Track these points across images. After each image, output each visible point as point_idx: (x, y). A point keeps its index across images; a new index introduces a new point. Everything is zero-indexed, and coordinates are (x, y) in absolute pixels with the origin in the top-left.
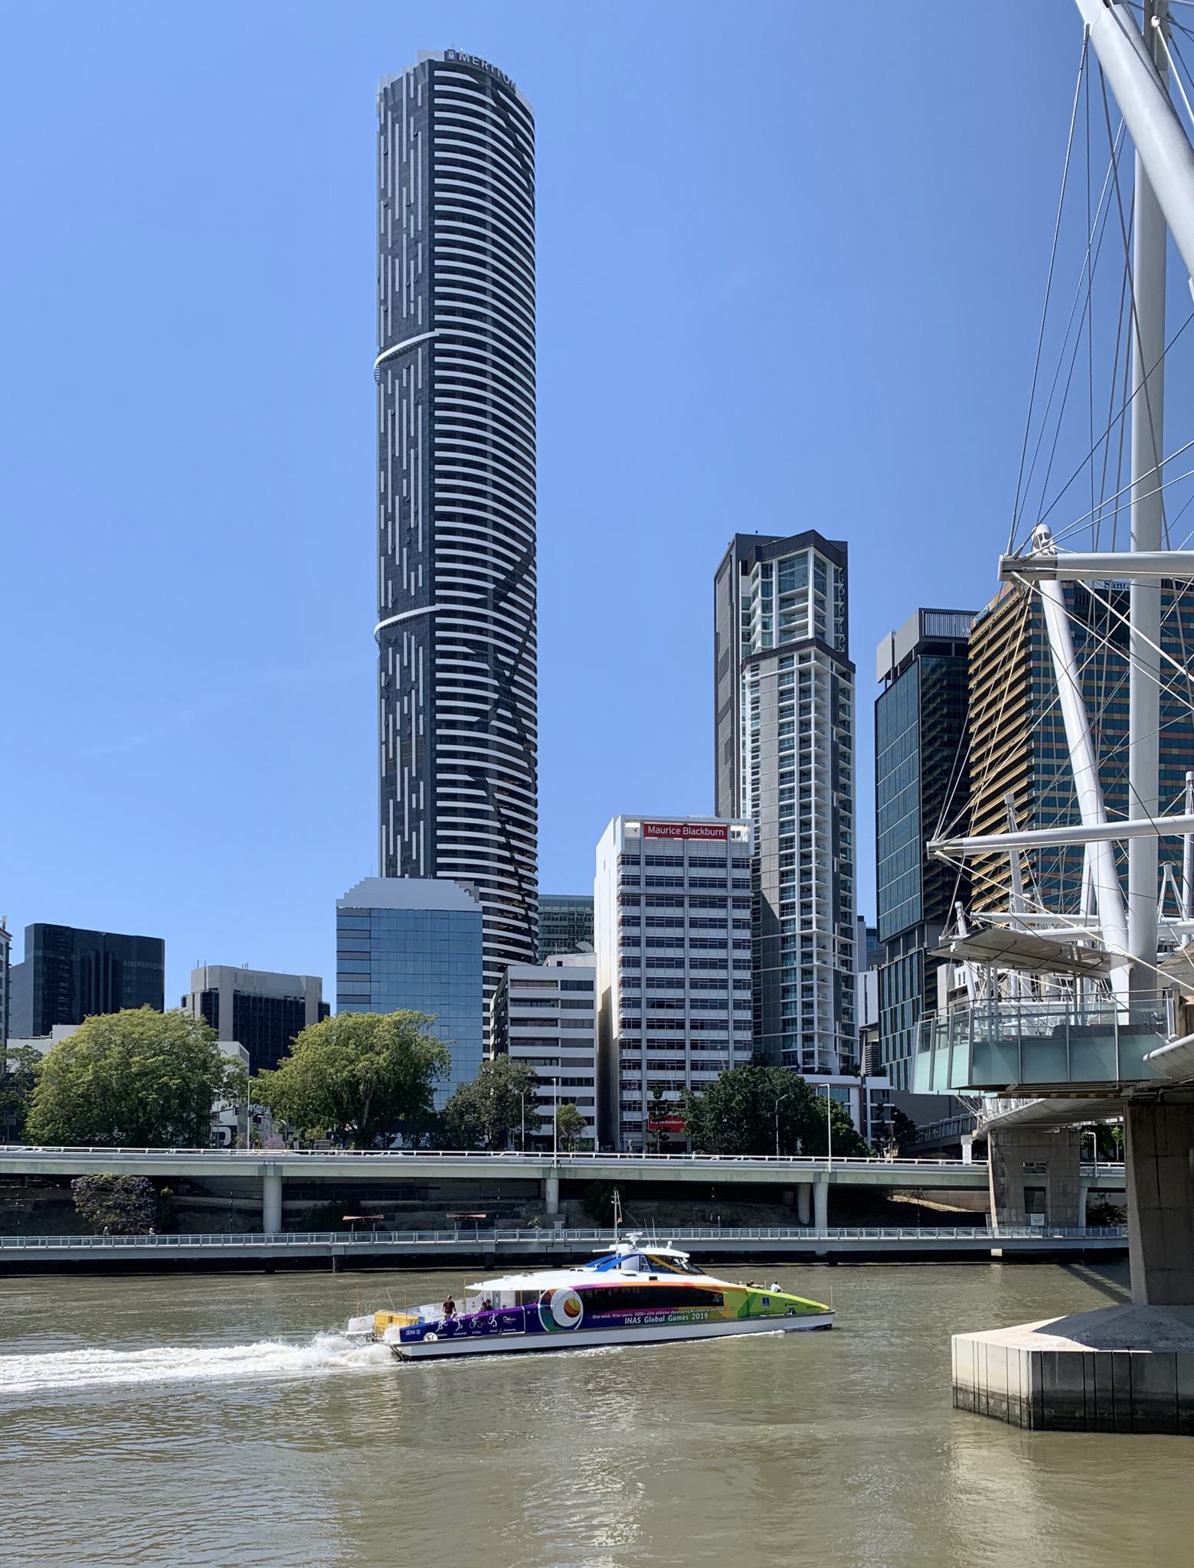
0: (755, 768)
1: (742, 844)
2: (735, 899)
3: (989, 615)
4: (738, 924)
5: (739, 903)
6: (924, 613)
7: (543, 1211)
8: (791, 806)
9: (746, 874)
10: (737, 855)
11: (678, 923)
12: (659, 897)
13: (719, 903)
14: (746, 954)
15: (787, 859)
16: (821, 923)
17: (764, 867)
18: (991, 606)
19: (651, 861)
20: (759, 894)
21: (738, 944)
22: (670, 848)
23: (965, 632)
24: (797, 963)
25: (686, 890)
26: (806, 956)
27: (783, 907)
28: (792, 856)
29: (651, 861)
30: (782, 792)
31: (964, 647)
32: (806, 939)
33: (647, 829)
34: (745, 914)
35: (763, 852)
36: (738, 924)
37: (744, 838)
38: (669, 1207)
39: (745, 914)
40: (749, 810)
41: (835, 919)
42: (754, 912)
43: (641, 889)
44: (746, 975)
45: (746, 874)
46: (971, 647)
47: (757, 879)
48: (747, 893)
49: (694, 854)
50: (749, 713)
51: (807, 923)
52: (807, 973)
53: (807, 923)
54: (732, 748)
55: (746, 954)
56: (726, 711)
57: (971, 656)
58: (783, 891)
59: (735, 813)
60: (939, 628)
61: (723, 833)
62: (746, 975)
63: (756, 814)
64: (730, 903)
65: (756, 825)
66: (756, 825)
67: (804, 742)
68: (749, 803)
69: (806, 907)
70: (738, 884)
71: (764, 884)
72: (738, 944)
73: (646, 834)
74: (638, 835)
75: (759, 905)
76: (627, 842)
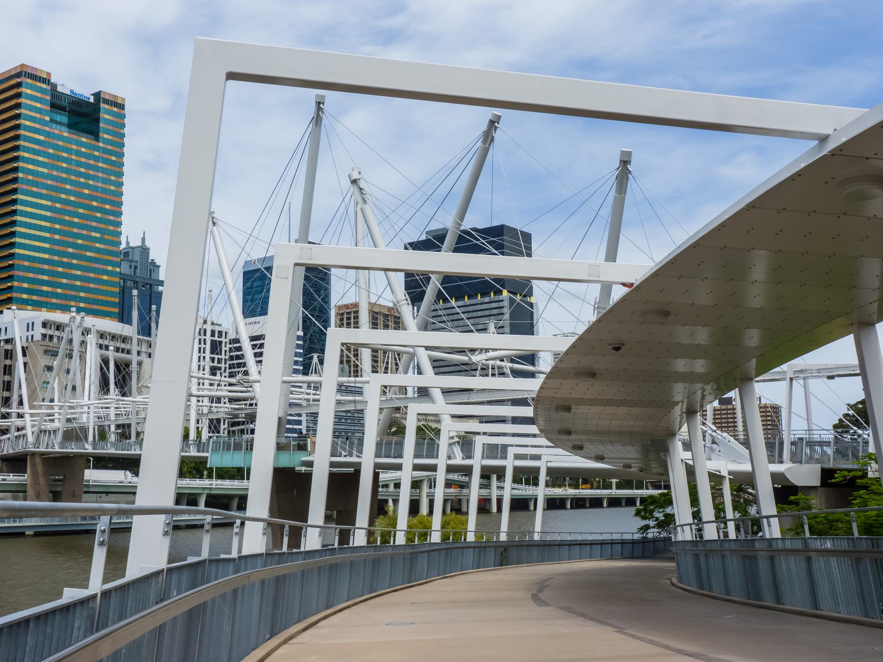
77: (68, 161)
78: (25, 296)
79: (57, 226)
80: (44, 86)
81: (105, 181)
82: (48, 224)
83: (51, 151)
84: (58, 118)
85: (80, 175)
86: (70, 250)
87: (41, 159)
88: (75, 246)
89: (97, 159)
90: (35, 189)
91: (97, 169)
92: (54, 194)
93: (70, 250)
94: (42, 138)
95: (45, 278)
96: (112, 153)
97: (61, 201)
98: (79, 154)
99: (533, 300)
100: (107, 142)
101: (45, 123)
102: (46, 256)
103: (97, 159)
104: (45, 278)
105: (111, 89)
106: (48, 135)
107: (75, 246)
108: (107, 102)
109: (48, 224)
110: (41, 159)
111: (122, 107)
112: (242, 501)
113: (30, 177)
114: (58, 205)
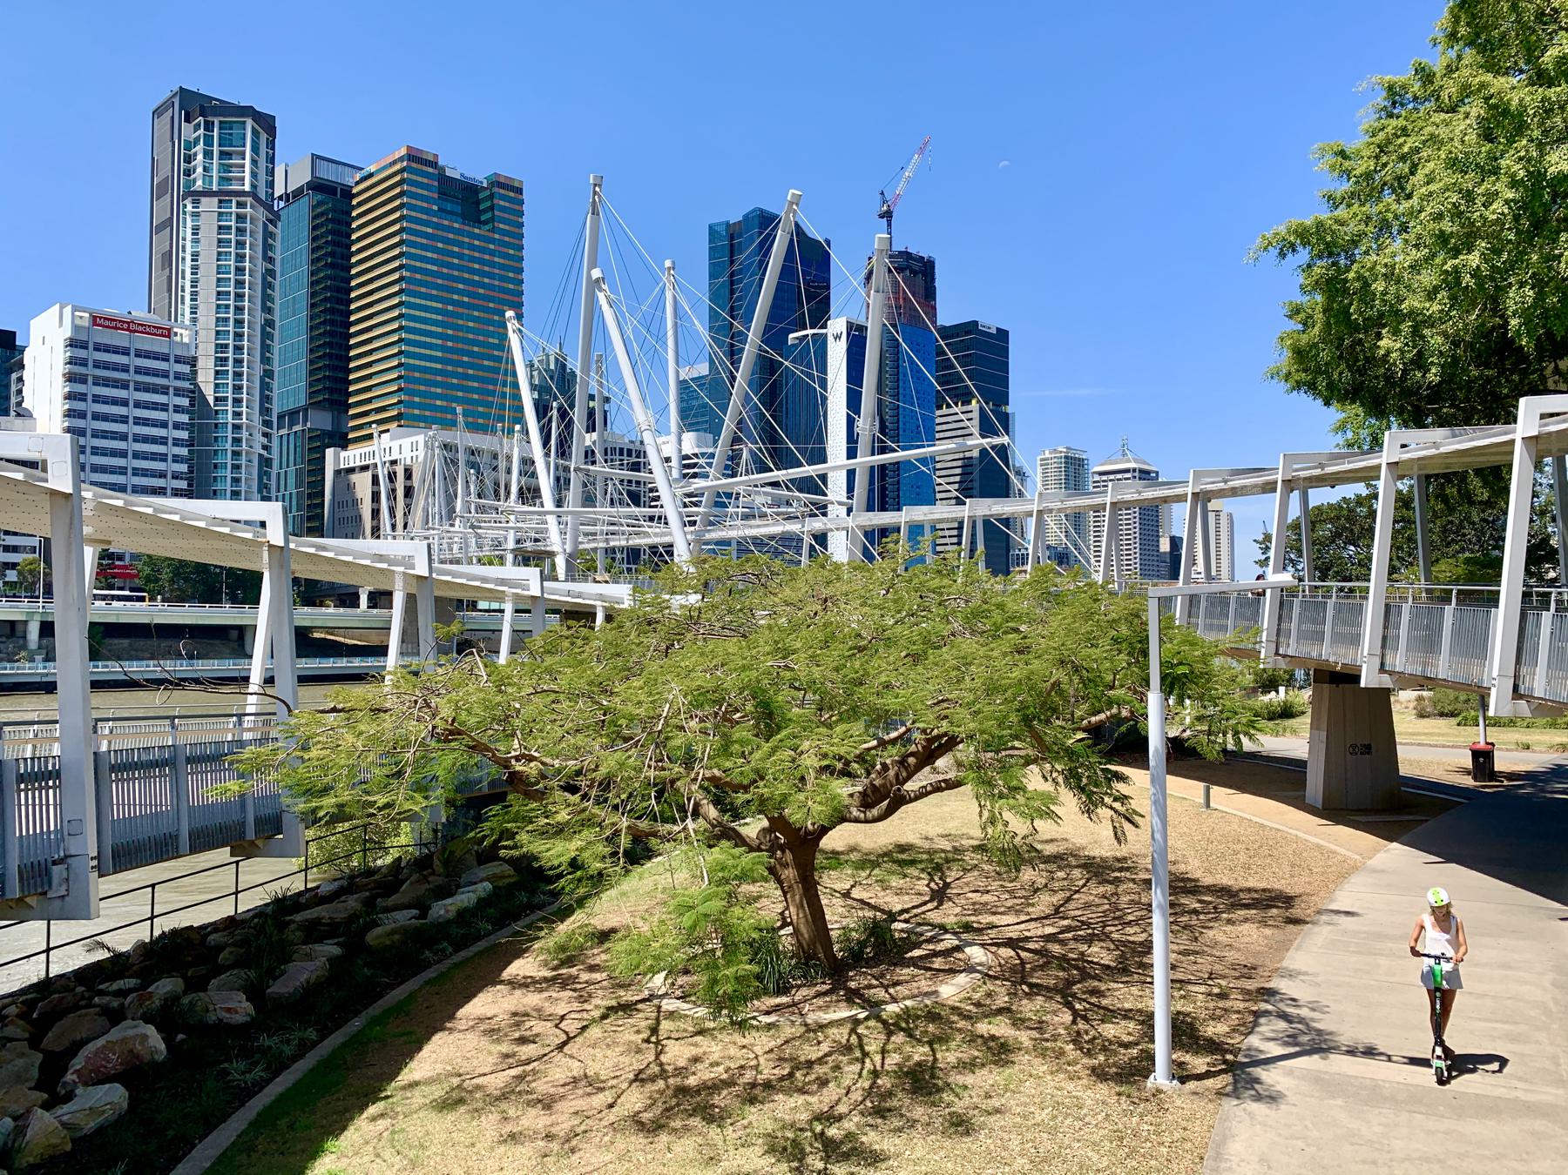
0: (194, 283)
1: (182, 344)
2: (176, 389)
3: (371, 175)
4: (178, 409)
5: (179, 392)
6: (315, 157)
7: (24, 647)
8: (227, 319)
9: (186, 369)
10: (179, 353)
11: (125, 403)
12: (106, 379)
13: (164, 390)
14: (184, 435)
15: (222, 361)
16: (250, 415)
17: (200, 363)
18: (373, 169)
19: (98, 348)
20: (196, 385)
21: (177, 426)
22: (120, 338)
23: (351, 182)
24: (228, 446)
25: (131, 376)
26: (237, 441)
27: (217, 399)
28: (226, 359)
29: (98, 348)
30: (218, 306)
31: (348, 194)
32: (237, 427)
33: (95, 320)
34: (185, 402)
35: (200, 352)
36: (178, 409)
37: (186, 340)
38: (141, 643)
39: (185, 402)
40: (188, 315)
41: (261, 414)
42: (192, 400)
43: (90, 371)
44: (184, 451)
45: (186, 369)
46: (354, 196)
47: (195, 373)
48: (186, 385)
49: (139, 346)
50: (189, 236)
51: (237, 415)
52: (236, 454)
53: (237, 415)
54: (167, 259)
55: (184, 435)
56: (165, 226)
57: (354, 202)
58: (217, 386)
59: (172, 312)
60: (328, 174)
61: (168, 333)
62: (184, 451)
63: (194, 320)
64: (171, 391)
65: (196, 332)
66: (196, 332)
67: (240, 270)
68: (187, 311)
69: (237, 402)
70: (178, 376)
71: (200, 378)
72: (177, 426)
73: (95, 324)
74: (86, 323)
75: (196, 395)
76: (76, 328)
77: (460, 256)
78: (417, 412)
79: (450, 332)
80: (431, 170)
81: (502, 279)
82: (439, 330)
83: (440, 245)
84: (449, 207)
85: (473, 271)
86: (465, 359)
87: (429, 255)
88: (470, 354)
89: (492, 253)
90: (423, 290)
91: (492, 264)
92: (445, 294)
93: (465, 359)
94: (430, 230)
95: (439, 391)
96: (508, 245)
97: (453, 303)
98: (472, 248)
99: (1009, 409)
100: (503, 233)
101: (434, 214)
102: (439, 366)
103: (492, 253)
104: (439, 391)
105: (508, 171)
106: (437, 226)
107: (470, 354)
108: (501, 185)
109: (439, 330)
110: (429, 255)
111: (520, 191)
112: (246, 679)
113: (418, 276)
114: (450, 308)
